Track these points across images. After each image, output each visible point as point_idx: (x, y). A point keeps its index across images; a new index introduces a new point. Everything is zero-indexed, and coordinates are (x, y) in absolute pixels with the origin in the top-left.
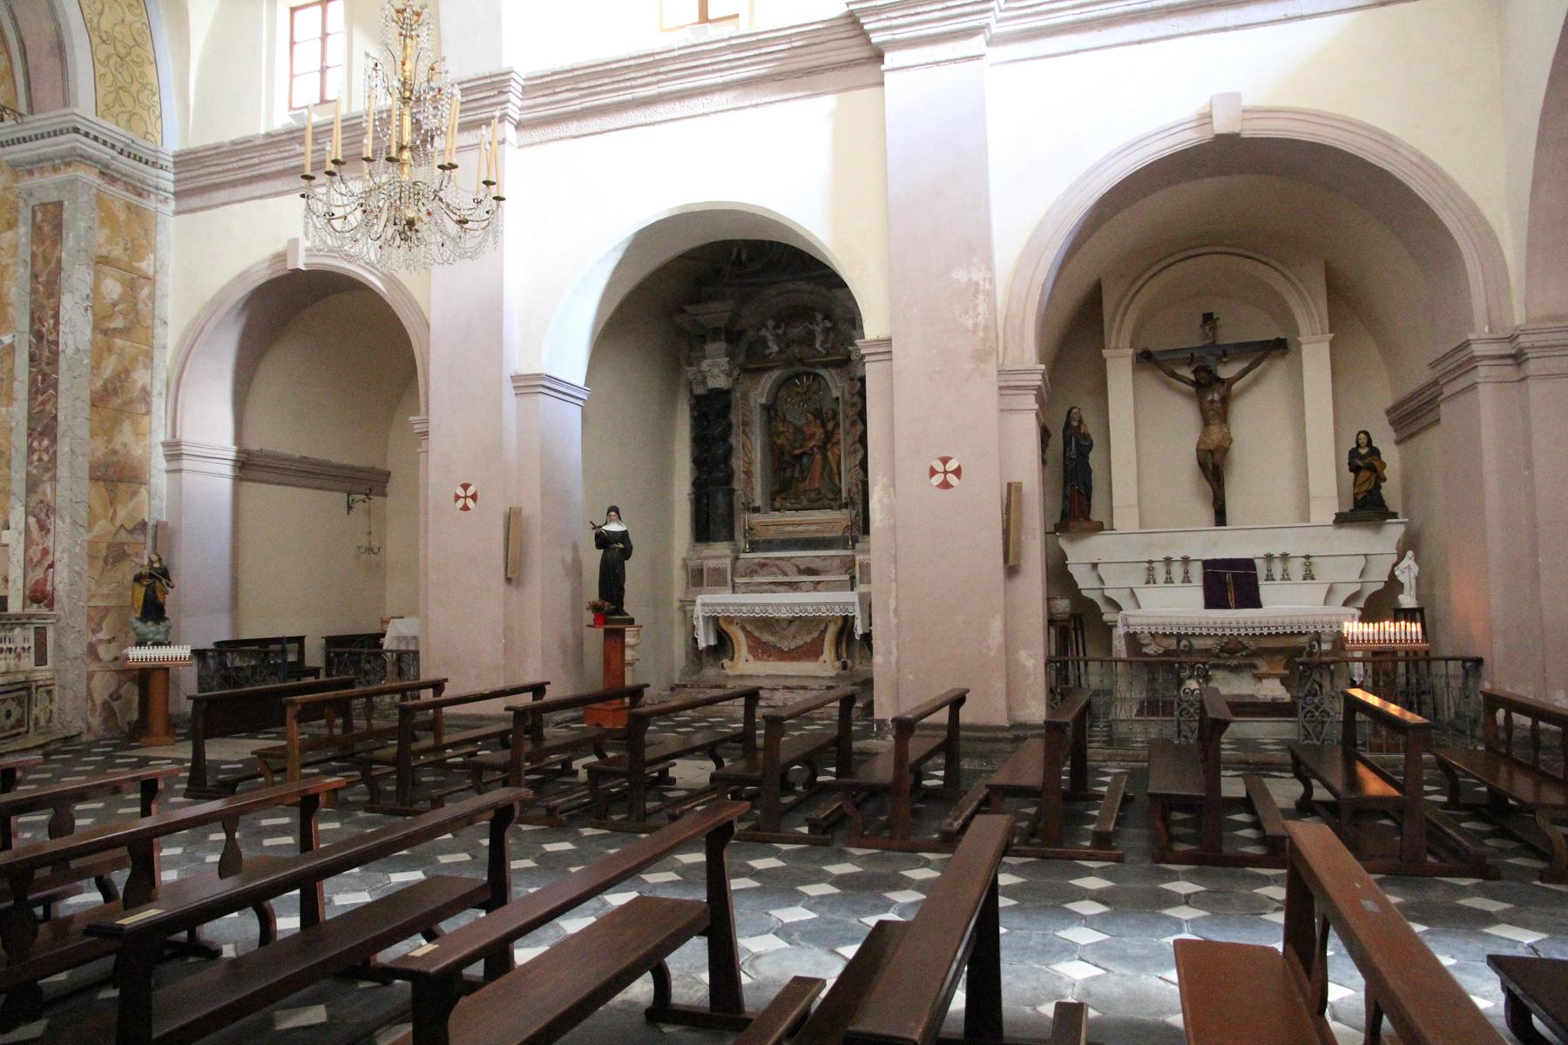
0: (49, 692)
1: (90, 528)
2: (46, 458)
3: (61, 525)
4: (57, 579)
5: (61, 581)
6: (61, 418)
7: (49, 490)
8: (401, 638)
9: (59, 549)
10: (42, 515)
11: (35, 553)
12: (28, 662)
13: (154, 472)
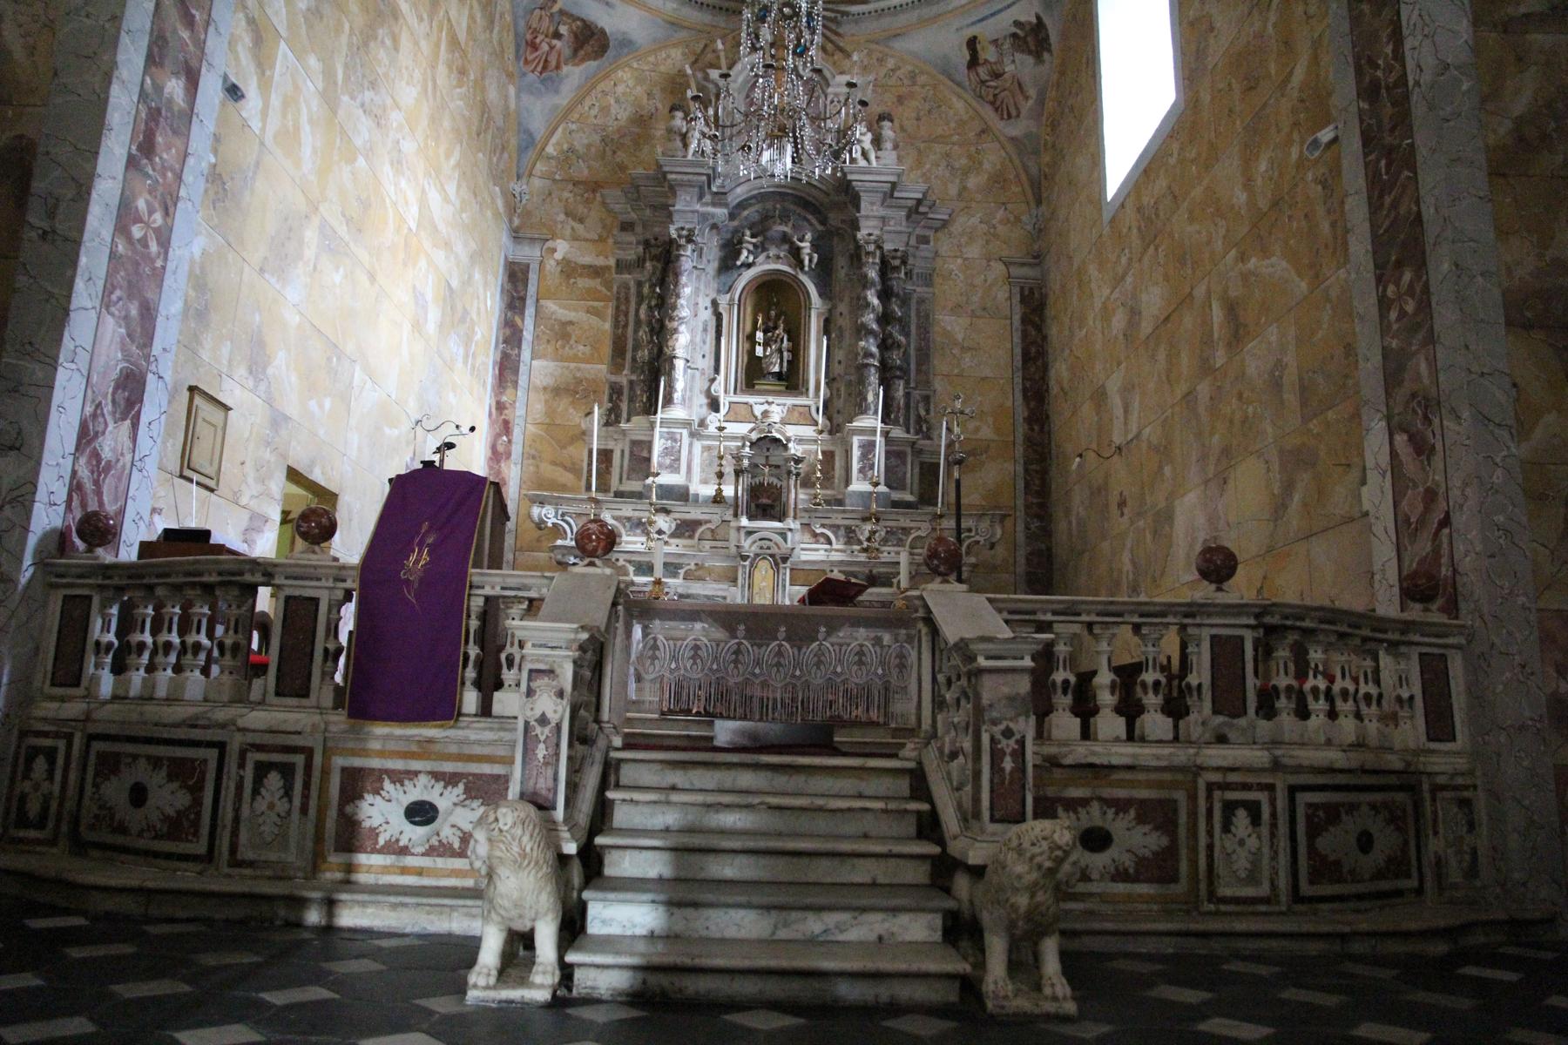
0: (1465, 804)
1: (1522, 430)
2: (1410, 307)
3: (1455, 430)
4: (1460, 548)
5: (1468, 548)
6: (1428, 212)
7: (1423, 367)
9: (1456, 482)
10: (1416, 419)
11: (1413, 505)
12: (1411, 731)
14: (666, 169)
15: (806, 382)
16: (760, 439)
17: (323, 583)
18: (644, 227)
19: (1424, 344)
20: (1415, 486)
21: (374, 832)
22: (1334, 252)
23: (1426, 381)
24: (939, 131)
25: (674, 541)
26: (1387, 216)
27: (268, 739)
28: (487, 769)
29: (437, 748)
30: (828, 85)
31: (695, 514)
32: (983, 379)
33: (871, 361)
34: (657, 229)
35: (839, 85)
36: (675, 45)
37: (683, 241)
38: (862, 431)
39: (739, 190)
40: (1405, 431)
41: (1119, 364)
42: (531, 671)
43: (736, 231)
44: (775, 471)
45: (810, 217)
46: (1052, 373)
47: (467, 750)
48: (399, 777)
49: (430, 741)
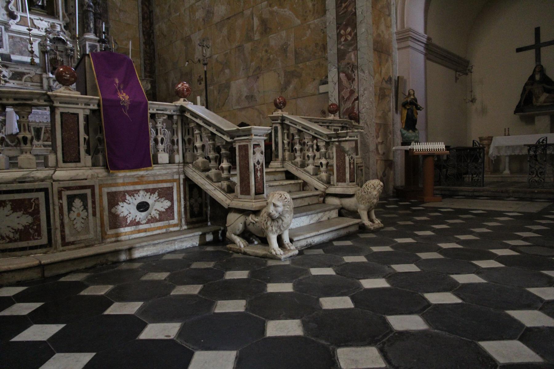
2: (349, 38)
4: (361, 107)
6: (359, 12)
7: (353, 56)
8: (498, 148)
9: (362, 89)
13: (394, 49)
15: (58, 13)
16: (54, 38)
17: (79, 106)
19: (353, 50)
20: (347, 88)
21: (125, 218)
22: (314, 13)
23: (353, 60)
25: (11, 81)
26: (343, 9)
27: (71, 184)
28: (165, 185)
29: (145, 179)
31: (21, 69)
32: (128, 24)
33: (91, 9)
38: (90, 40)
40: (344, 73)
41: (199, 30)
42: (254, 145)
44: (60, 53)
46: (156, 27)
47: (157, 179)
48: (132, 193)
49: (142, 176)
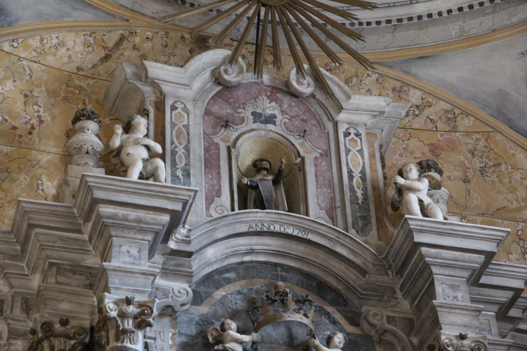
14: (99, 194)
18: (27, 309)
24: (500, 201)
30: (340, 108)
34: (65, 306)
35: (357, 110)
36: (70, 29)
37: (129, 324)
39: (211, 252)
43: (204, 323)
45: (330, 309)
